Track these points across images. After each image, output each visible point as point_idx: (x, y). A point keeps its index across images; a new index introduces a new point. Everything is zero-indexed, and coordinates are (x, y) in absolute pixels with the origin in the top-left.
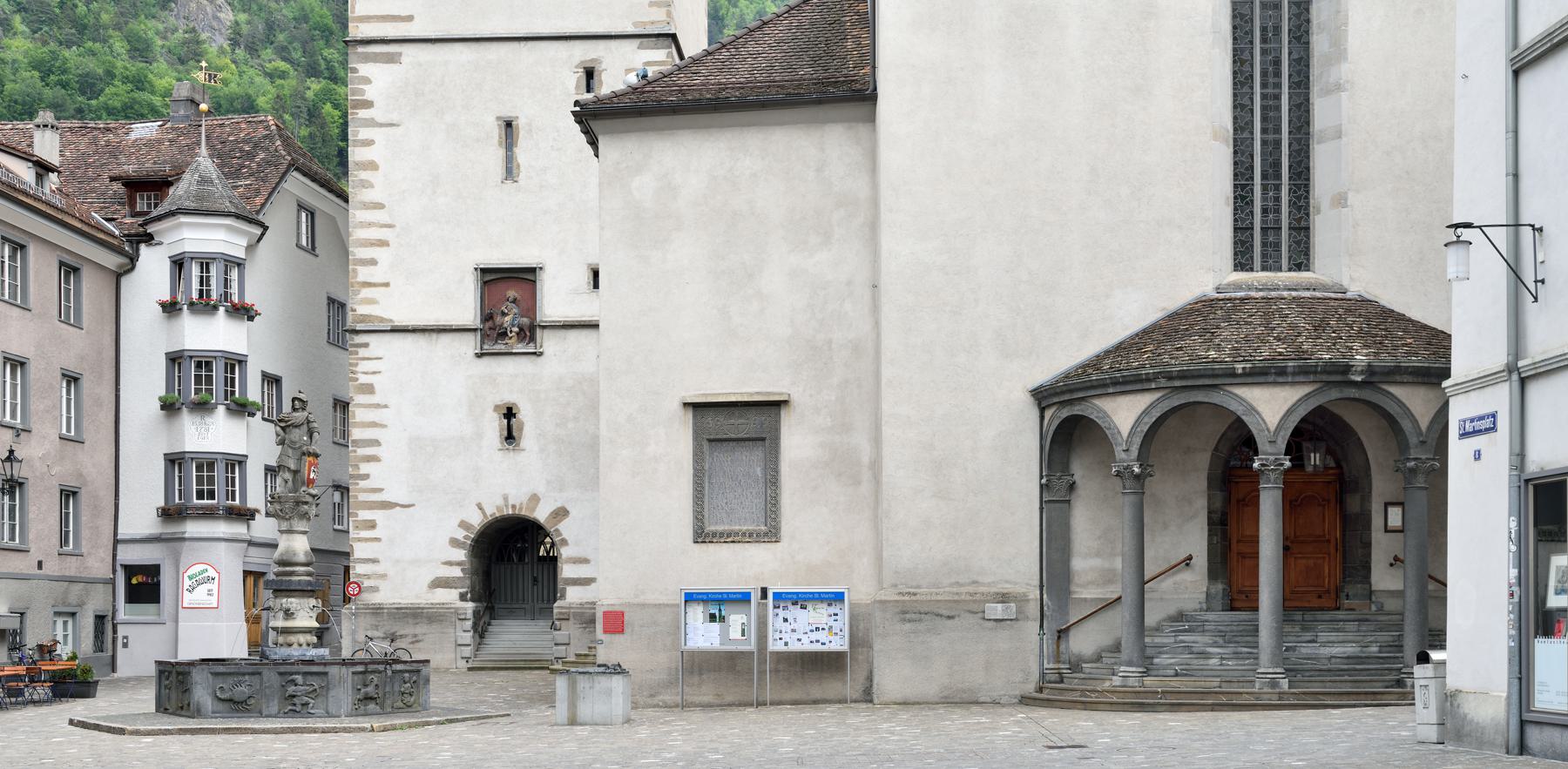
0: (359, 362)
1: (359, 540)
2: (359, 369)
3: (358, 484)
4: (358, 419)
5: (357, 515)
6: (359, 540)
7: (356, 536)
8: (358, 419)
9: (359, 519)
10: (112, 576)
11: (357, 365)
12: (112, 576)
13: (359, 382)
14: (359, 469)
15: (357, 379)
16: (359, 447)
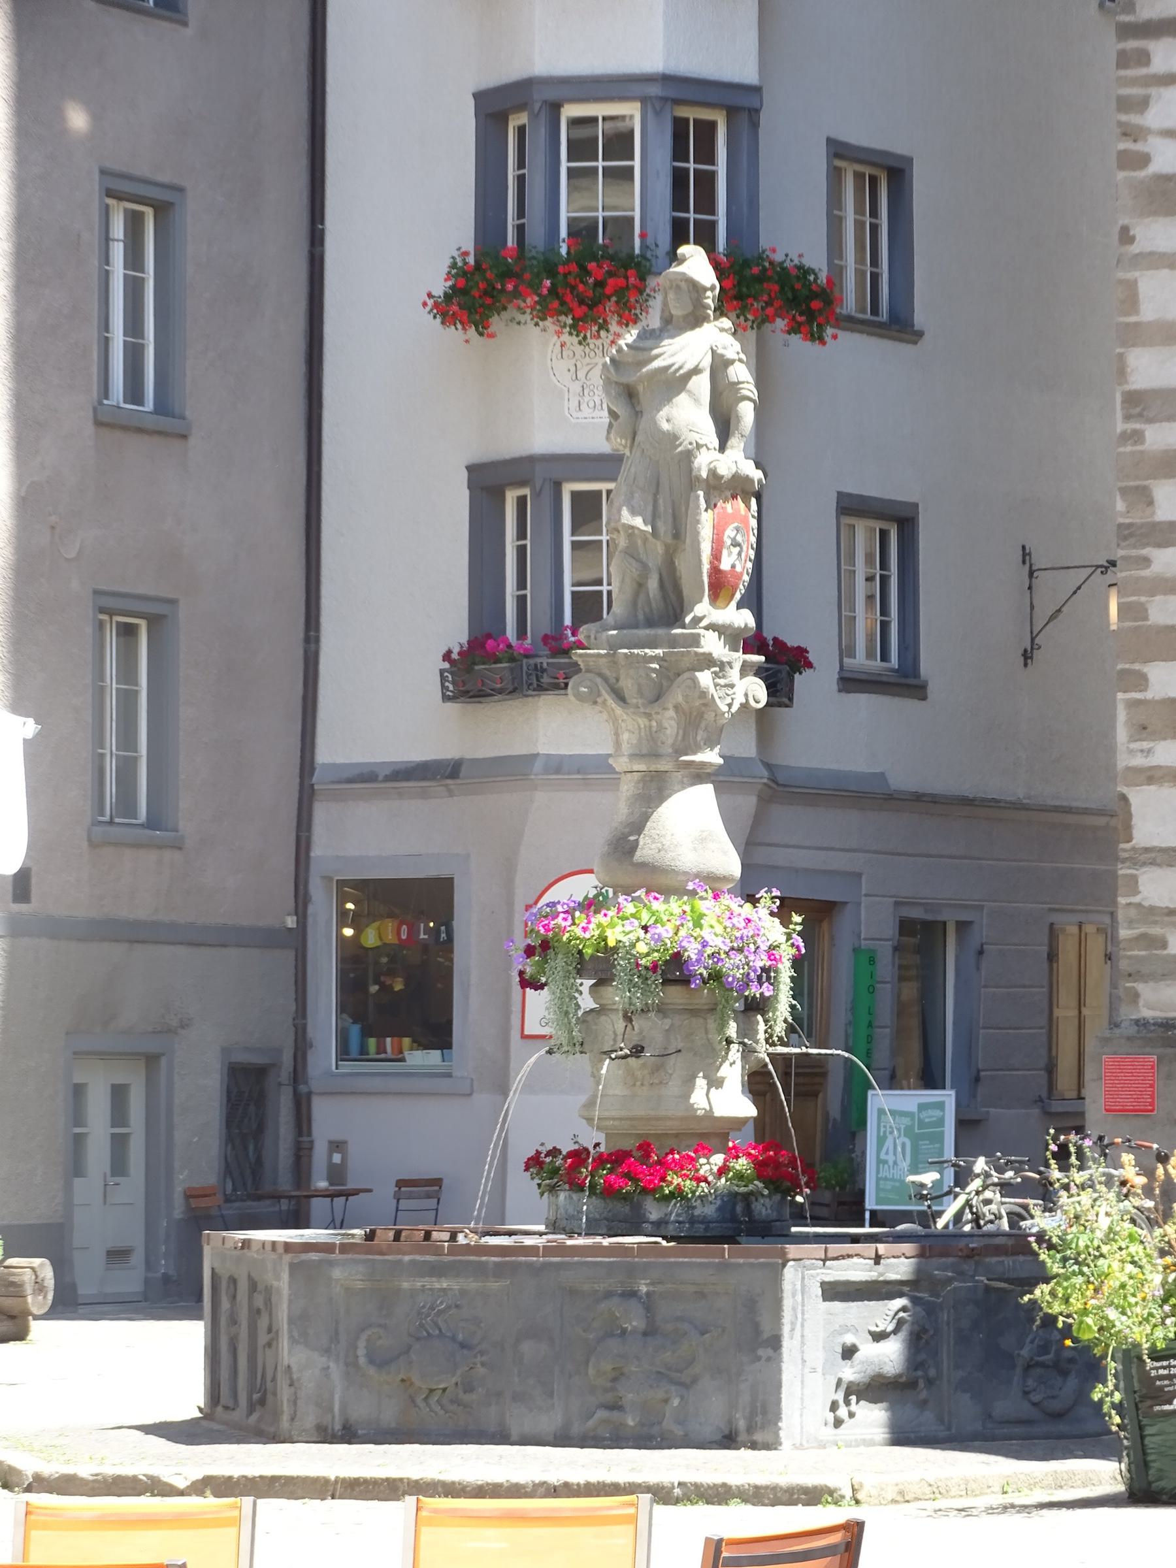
0: (1153, 91)
1: (1152, 776)
2: (1153, 118)
3: (1146, 561)
4: (1148, 313)
5: (1141, 681)
6: (1152, 776)
7: (1139, 761)
8: (1148, 313)
9: (1149, 695)
10: (291, 922)
11: (1143, 104)
12: (291, 922)
13: (1155, 167)
14: (1151, 503)
15: (1144, 160)
16: (1150, 421)
